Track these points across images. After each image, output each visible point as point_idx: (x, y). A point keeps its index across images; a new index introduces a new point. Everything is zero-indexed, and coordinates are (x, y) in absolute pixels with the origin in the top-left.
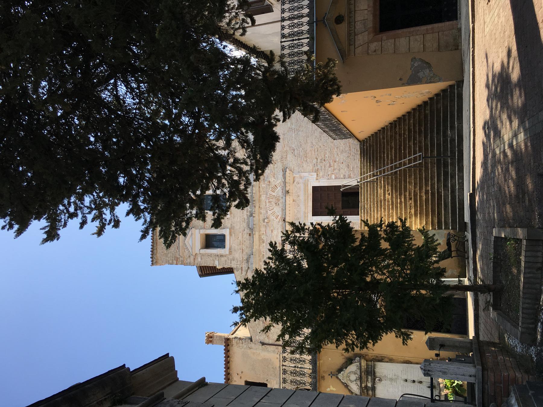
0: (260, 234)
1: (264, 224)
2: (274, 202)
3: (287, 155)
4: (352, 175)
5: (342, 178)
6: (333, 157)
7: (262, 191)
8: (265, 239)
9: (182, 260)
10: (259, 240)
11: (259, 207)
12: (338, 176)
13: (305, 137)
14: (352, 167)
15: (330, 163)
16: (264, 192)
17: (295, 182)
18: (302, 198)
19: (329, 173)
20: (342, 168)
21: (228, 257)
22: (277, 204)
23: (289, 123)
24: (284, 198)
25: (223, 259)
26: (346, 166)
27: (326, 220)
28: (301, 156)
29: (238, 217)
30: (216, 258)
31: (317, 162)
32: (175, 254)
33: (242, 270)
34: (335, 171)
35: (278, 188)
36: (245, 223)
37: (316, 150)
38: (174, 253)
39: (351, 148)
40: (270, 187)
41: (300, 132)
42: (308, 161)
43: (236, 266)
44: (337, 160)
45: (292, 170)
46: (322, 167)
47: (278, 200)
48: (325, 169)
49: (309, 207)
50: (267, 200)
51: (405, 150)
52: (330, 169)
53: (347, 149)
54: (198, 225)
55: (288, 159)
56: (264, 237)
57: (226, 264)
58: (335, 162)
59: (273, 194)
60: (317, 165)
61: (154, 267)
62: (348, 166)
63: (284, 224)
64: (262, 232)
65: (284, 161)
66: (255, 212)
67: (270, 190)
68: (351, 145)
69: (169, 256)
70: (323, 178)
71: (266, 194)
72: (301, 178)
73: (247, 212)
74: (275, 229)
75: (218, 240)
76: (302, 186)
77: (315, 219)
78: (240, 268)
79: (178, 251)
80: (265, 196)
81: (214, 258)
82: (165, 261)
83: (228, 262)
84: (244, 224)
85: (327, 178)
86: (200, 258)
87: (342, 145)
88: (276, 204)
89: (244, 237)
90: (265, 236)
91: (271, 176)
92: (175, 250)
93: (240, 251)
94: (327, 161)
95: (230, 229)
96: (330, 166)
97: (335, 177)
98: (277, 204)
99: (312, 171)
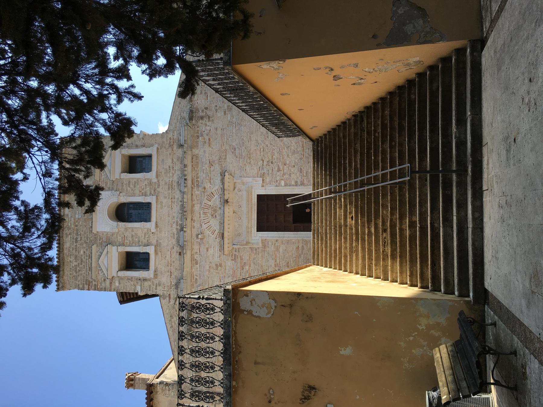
0: (193, 253)
1: (198, 240)
2: (210, 213)
3: (226, 156)
4: (305, 182)
5: (293, 185)
6: (283, 158)
8: (198, 259)
10: (191, 261)
11: (192, 219)
12: (288, 182)
13: (249, 134)
14: (305, 172)
15: (279, 166)
16: (197, 200)
17: (236, 190)
18: (244, 209)
19: (278, 178)
20: (293, 173)
21: (153, 282)
22: (214, 216)
23: (229, 116)
24: (222, 208)
25: (146, 284)
26: (298, 170)
27: (274, 237)
28: (243, 157)
29: (165, 232)
30: (137, 283)
31: (263, 165)
32: (87, 277)
33: (170, 298)
34: (284, 176)
35: (216, 196)
36: (174, 238)
37: (262, 150)
39: (305, 148)
40: (206, 194)
41: (242, 127)
42: (252, 163)
43: (163, 293)
44: (288, 162)
45: (233, 174)
46: (268, 171)
47: (215, 211)
48: (272, 174)
50: (202, 211)
51: (376, 155)
52: (278, 173)
53: (300, 149)
55: (228, 160)
56: (197, 257)
57: (150, 290)
58: (285, 165)
59: (209, 203)
60: (263, 169)
61: (61, 292)
62: (301, 171)
63: (222, 241)
64: (195, 251)
65: (223, 163)
66: (186, 225)
67: (205, 199)
68: (304, 143)
69: (79, 279)
70: (270, 184)
71: (200, 202)
72: (243, 184)
73: (177, 225)
74: (211, 246)
75: (141, 259)
76: (244, 193)
77: (260, 235)
78: (168, 295)
79: (90, 272)
80: (199, 205)
81: (135, 283)
82: (74, 285)
84: (173, 240)
85: (275, 184)
86: (118, 282)
87: (294, 144)
88: (212, 215)
90: (198, 256)
91: (207, 181)
92: (87, 272)
94: (276, 164)
95: (155, 247)
96: (279, 170)
97: (285, 183)
98: (214, 216)
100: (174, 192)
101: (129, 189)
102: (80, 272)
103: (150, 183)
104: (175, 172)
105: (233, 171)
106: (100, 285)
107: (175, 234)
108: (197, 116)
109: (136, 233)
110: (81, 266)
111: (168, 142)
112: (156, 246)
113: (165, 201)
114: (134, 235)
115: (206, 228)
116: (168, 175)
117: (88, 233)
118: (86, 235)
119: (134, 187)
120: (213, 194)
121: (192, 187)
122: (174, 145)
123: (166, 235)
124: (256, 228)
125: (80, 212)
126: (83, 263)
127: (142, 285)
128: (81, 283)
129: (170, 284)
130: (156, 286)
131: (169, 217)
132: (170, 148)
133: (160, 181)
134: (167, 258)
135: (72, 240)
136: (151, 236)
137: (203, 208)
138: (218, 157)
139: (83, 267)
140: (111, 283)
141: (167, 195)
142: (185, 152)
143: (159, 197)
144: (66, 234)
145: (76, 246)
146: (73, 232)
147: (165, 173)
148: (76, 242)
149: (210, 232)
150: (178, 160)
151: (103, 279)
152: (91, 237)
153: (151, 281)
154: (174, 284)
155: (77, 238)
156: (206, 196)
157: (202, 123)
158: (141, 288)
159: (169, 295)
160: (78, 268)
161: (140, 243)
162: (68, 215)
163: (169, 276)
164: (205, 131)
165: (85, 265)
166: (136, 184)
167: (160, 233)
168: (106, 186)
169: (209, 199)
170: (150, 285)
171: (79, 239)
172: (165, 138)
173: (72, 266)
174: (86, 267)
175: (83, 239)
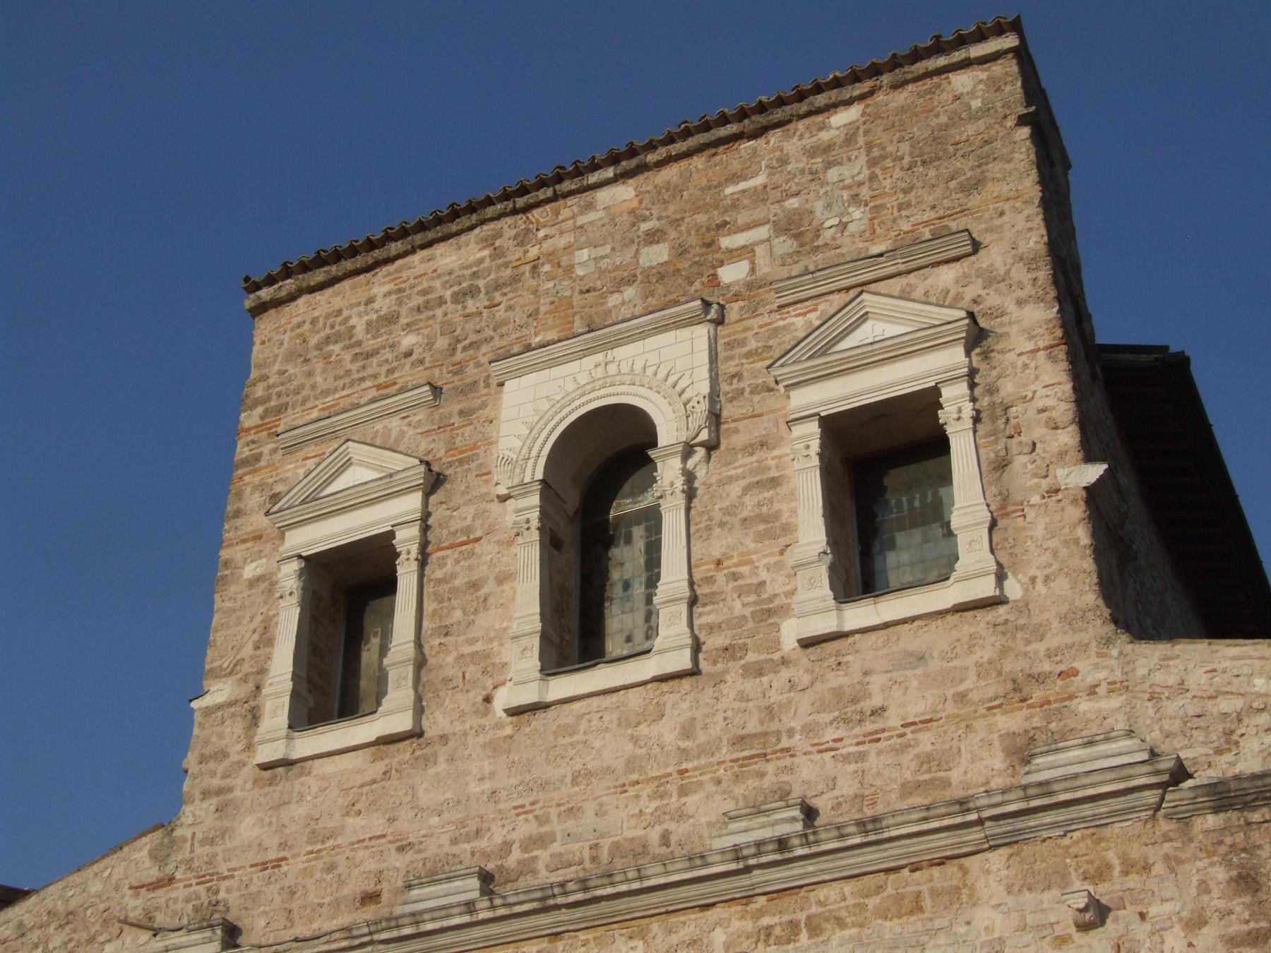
7: (674, 939)
9: (257, 458)
29: (492, 775)
33: (155, 886)
36: (454, 842)
38: (305, 393)
54: (457, 500)
57: (203, 760)
69: (291, 371)
78: (170, 869)
79: (315, 414)
81: (246, 668)
83: (213, 774)
84: (445, 840)
86: (259, 572)
89: (361, 853)
93: (272, 842)
100: (719, 782)
101: (736, 489)
102: (319, 366)
103: (770, 613)
104: (847, 759)
106: (257, 479)
107: (483, 843)
108: (1256, 837)
109: (491, 600)
110: (347, 357)
111: (1046, 667)
112: (416, 734)
113: (666, 731)
114: (484, 591)
116: (826, 717)
117: (497, 342)
118: (488, 332)
119: (745, 520)
121: (749, 898)
122: (1025, 712)
123: (474, 788)
125: (603, 264)
126: (359, 364)
127: (232, 710)
128: (274, 386)
129: (223, 868)
130: (220, 792)
131: (575, 781)
132: (1001, 691)
133: (785, 673)
134: (351, 821)
135: (467, 273)
136: (471, 695)
139: (341, 372)
140: (258, 538)
141: (702, 737)
142: (961, 802)
143: (686, 683)
144: (499, 234)
145: (441, 301)
146: (506, 265)
147: (838, 692)
148: (459, 298)
150: (926, 760)
151: (279, 488)
152: (478, 365)
153: (243, 757)
154: (222, 895)
155: (473, 292)
157: (1204, 888)
158: (219, 707)
159: (171, 879)
160: (336, 348)
161: (436, 642)
162: (590, 206)
163: (260, 859)
164: (1147, 927)
165: (347, 380)
166: (762, 527)
167: (484, 746)
168: (748, 355)
170: (225, 754)
171: (471, 305)
172: (1069, 639)
173: (349, 318)
174: (340, 383)
175: (470, 325)
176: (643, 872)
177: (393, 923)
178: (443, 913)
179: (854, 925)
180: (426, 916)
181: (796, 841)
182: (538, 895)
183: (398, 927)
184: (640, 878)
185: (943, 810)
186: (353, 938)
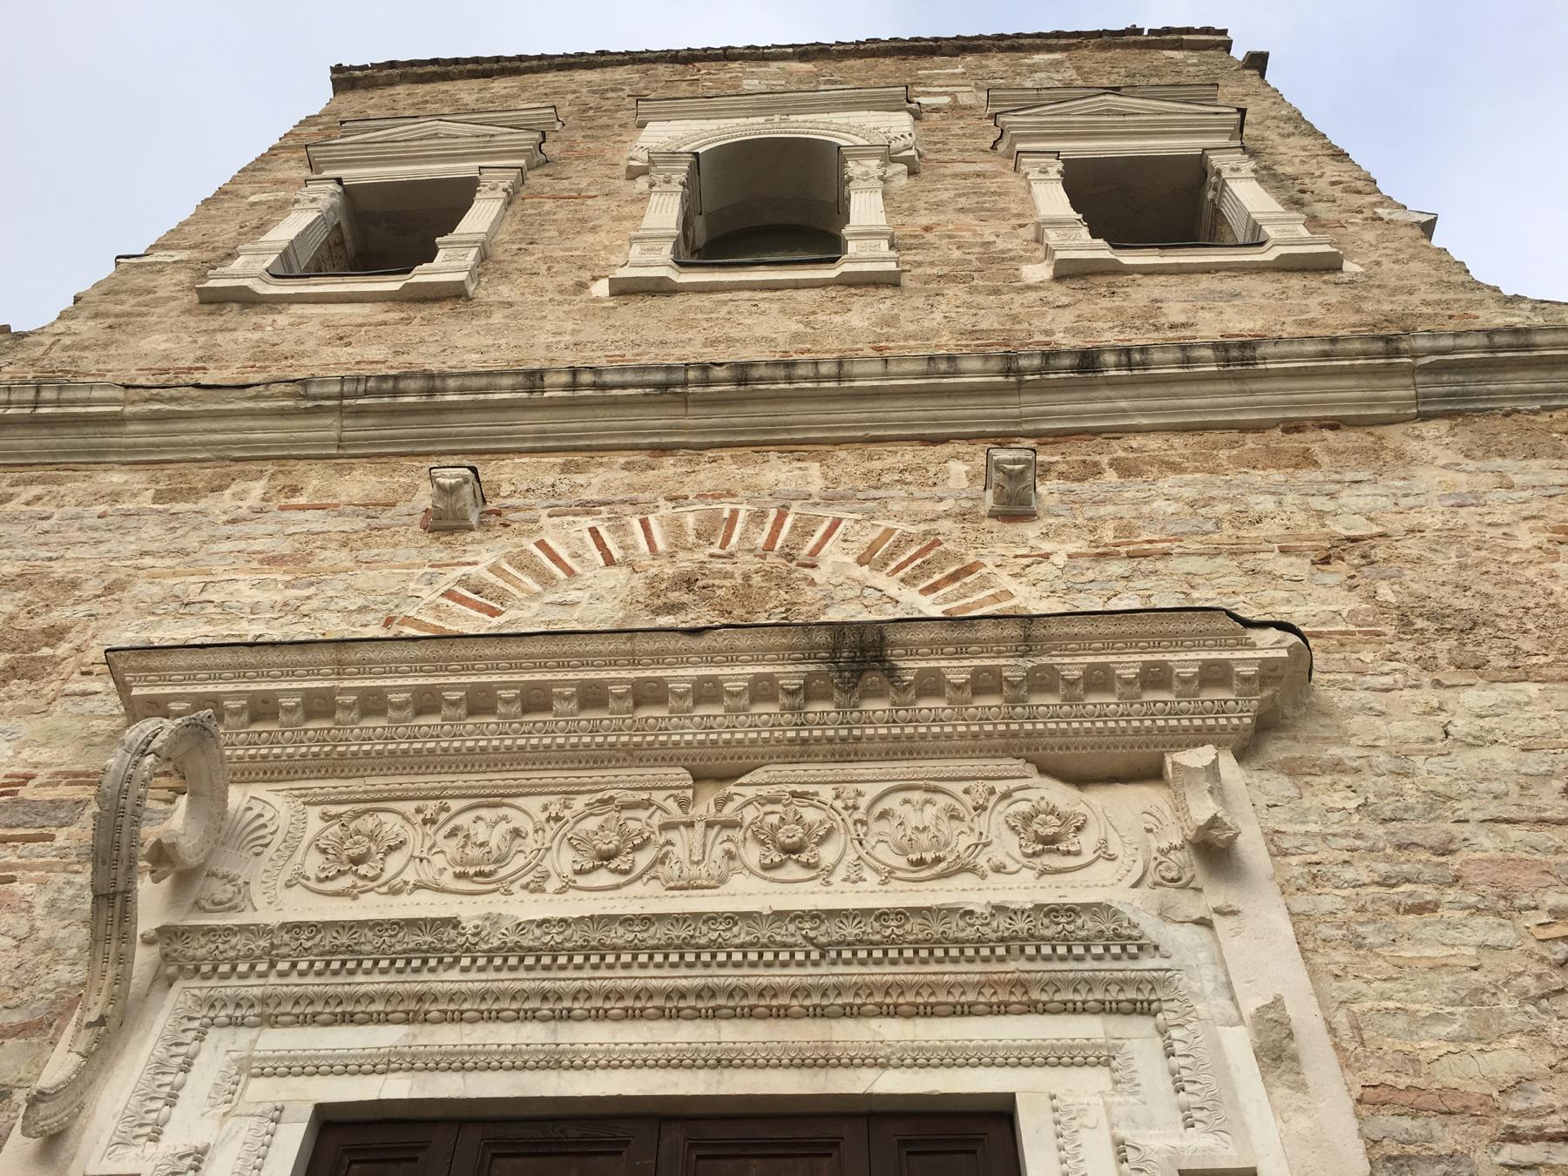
40: (945, 525)
45: (1277, 750)
49: (533, 1035)
55: (1477, 697)
91: (1108, 535)
99: (1374, 1076)
105: (1335, 751)
115: (541, 545)
120: (954, 578)
124: (397, 1087)
137: (781, 517)
138: (1462, 603)
149: (494, 569)
156: (924, 527)
169: (891, 555)
176: (847, 368)
177: (390, 385)
178: (483, 381)
179: (1196, 470)
180: (452, 383)
181: (1110, 358)
182: (659, 377)
183: (395, 393)
184: (839, 378)
185: (1357, 346)
186: (306, 397)
